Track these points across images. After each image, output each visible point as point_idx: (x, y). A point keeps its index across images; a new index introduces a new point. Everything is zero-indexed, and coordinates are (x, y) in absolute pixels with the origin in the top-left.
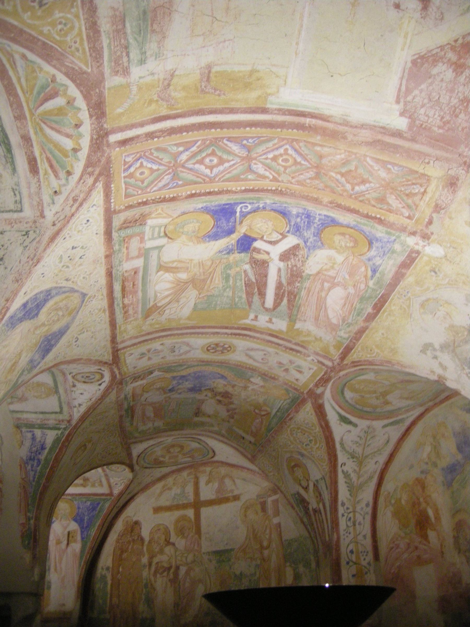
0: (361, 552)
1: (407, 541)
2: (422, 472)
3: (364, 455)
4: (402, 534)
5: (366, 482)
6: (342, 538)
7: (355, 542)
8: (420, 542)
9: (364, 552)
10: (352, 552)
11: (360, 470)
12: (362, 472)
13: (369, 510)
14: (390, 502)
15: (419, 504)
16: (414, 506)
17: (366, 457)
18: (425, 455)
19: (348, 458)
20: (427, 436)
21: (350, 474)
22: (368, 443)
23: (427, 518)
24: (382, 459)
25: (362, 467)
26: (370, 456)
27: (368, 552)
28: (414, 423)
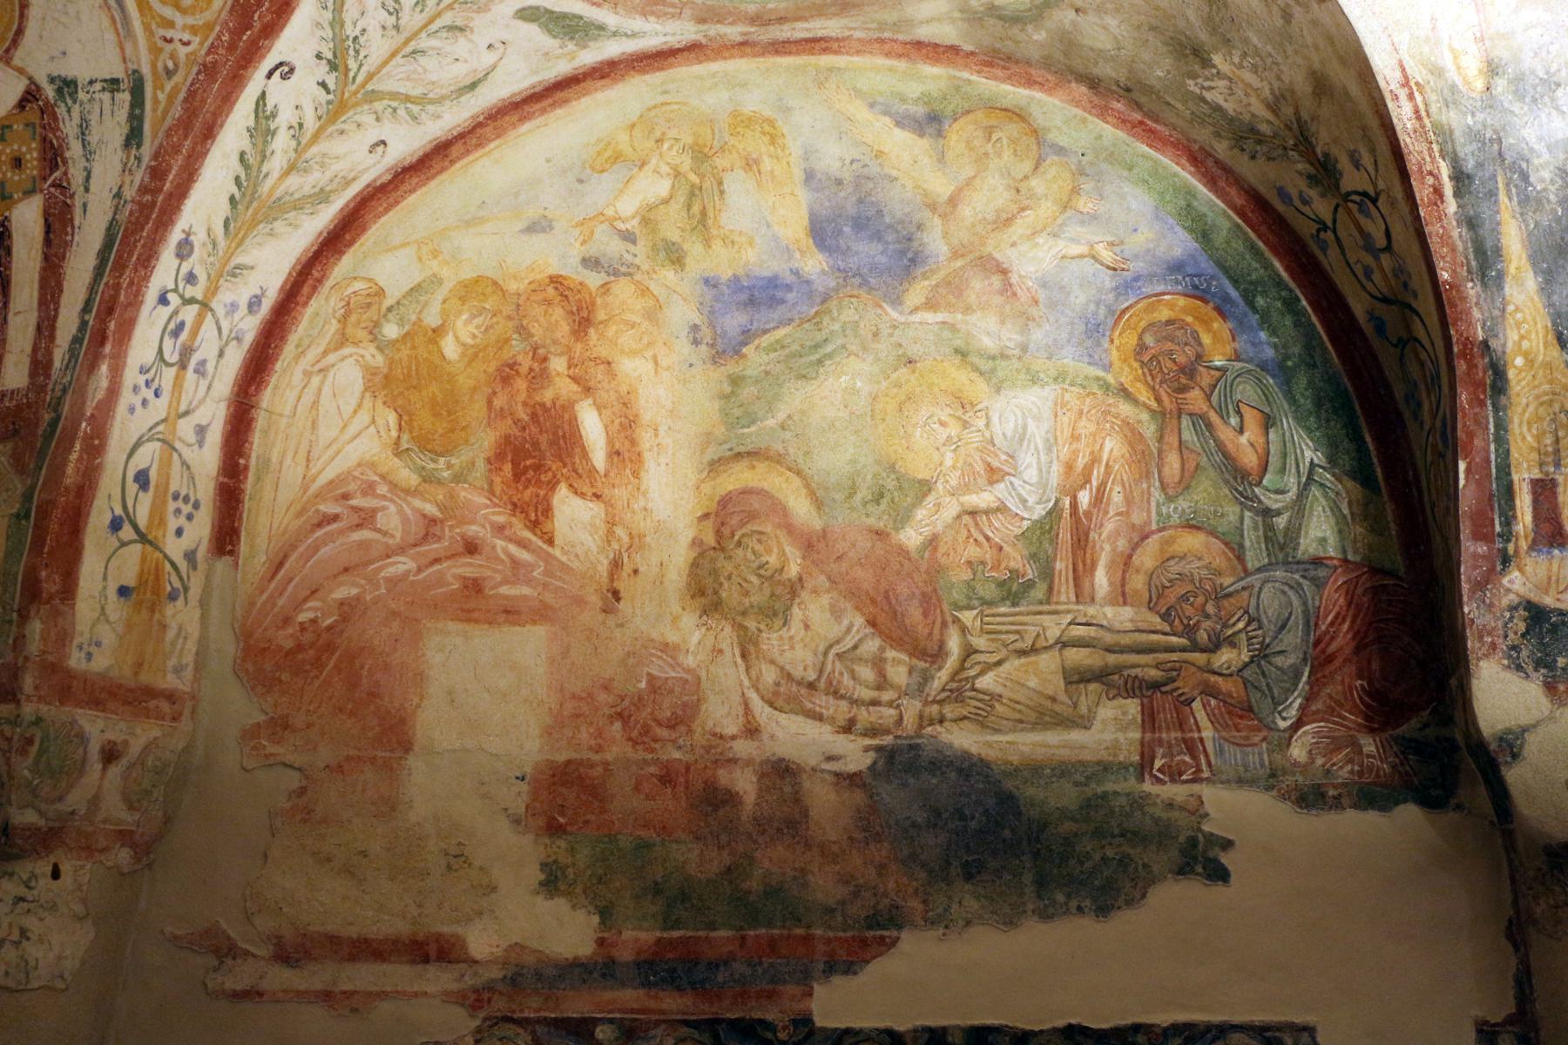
0: (176, 497)
1: (431, 509)
2: (591, 263)
3: (369, 87)
4: (406, 475)
5: (297, 206)
6: (126, 398)
7: (163, 441)
8: (500, 529)
9: (186, 499)
10: (142, 479)
11: (316, 137)
12: (314, 150)
13: (250, 326)
14: (374, 331)
15: (540, 376)
16: (506, 380)
17: (373, 96)
18: (628, 206)
19: (319, 56)
20: (659, 141)
21: (274, 133)
22: (424, 42)
23: (567, 441)
24: (406, 142)
25: (331, 129)
26: (378, 106)
27: (196, 506)
28: (607, 71)
